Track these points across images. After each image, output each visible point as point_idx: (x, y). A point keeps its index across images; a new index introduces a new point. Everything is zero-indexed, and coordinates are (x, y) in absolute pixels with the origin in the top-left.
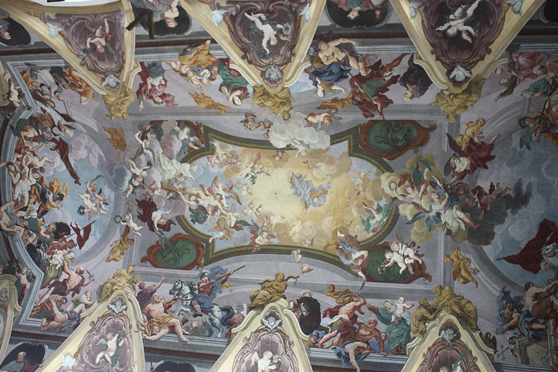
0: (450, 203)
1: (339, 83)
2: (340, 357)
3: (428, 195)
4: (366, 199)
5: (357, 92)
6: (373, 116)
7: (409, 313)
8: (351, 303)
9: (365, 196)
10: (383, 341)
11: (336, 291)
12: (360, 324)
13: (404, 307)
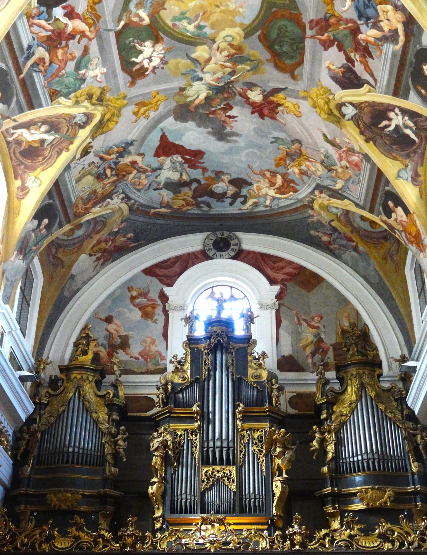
0: (213, 87)
1: (353, 8)
2: (27, 50)
3: (220, 69)
4: (211, 13)
5: (340, 22)
6: (311, 28)
7: (92, 82)
8: (87, 28)
9: (215, 12)
10: (57, 76)
11: (96, 7)
12: (67, 46)
13: (97, 76)
